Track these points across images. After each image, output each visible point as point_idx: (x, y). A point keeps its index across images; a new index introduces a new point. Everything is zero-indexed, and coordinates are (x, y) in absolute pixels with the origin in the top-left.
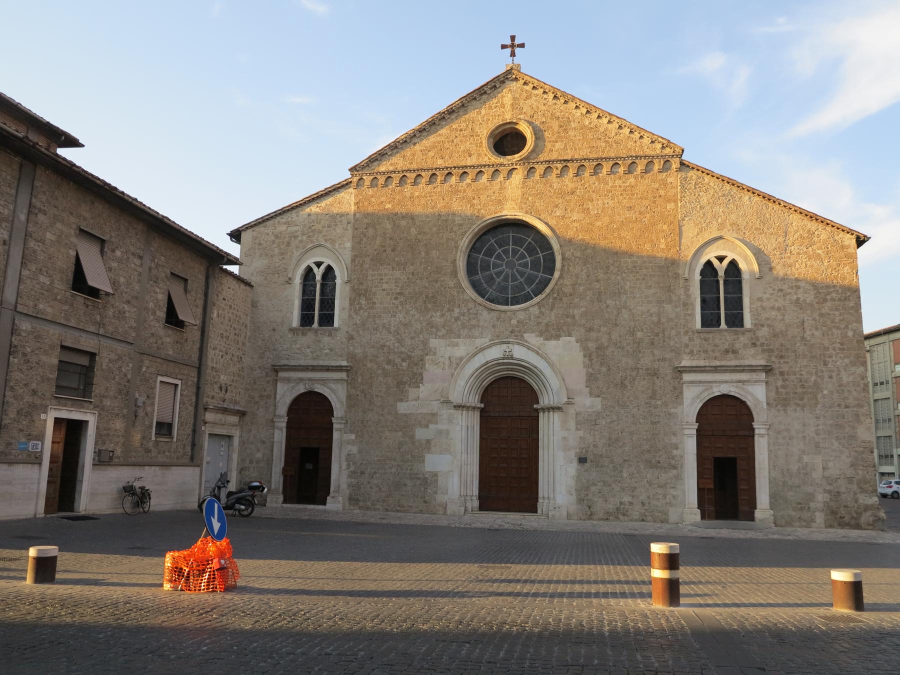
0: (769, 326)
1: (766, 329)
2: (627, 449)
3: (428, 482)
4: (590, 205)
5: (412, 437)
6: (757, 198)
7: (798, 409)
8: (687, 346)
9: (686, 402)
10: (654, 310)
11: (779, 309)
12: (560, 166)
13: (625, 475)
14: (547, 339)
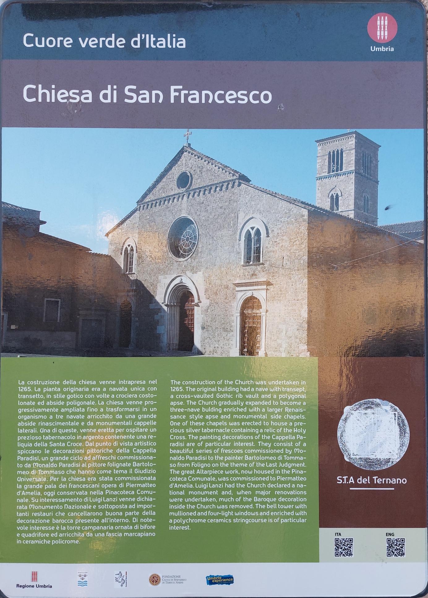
1: (268, 262)
2: (217, 322)
4: (208, 208)
6: (269, 195)
12: (198, 191)
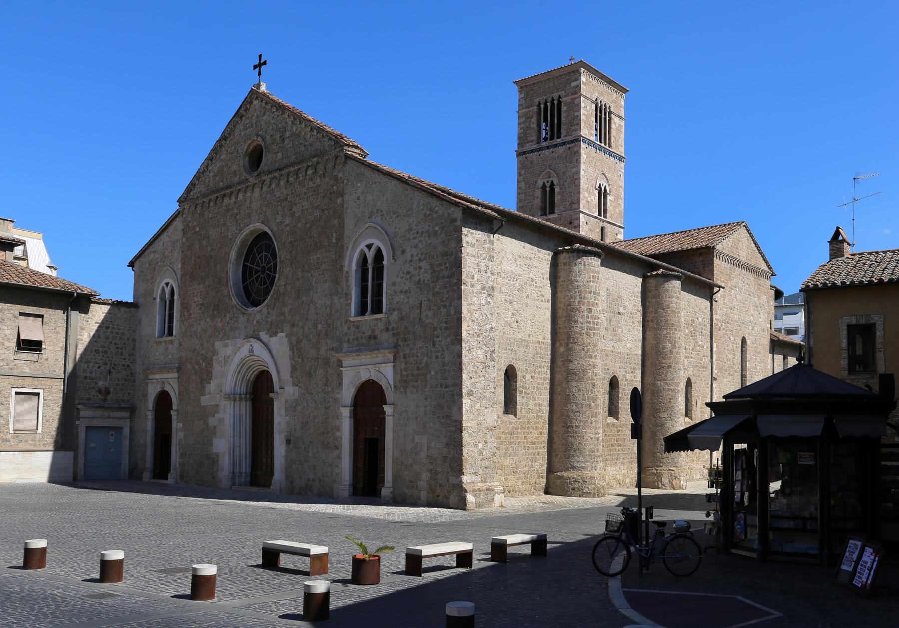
0: (399, 309)
1: (396, 313)
2: (312, 431)
3: (214, 460)
5: (207, 424)
7: (414, 390)
8: (346, 334)
9: (345, 387)
10: (328, 303)
11: (406, 292)
13: (310, 455)
14: (271, 336)
